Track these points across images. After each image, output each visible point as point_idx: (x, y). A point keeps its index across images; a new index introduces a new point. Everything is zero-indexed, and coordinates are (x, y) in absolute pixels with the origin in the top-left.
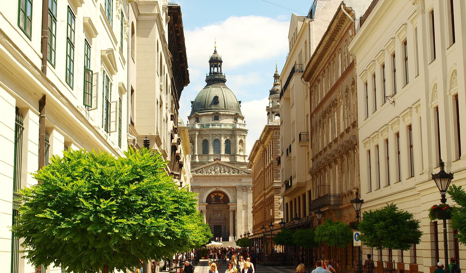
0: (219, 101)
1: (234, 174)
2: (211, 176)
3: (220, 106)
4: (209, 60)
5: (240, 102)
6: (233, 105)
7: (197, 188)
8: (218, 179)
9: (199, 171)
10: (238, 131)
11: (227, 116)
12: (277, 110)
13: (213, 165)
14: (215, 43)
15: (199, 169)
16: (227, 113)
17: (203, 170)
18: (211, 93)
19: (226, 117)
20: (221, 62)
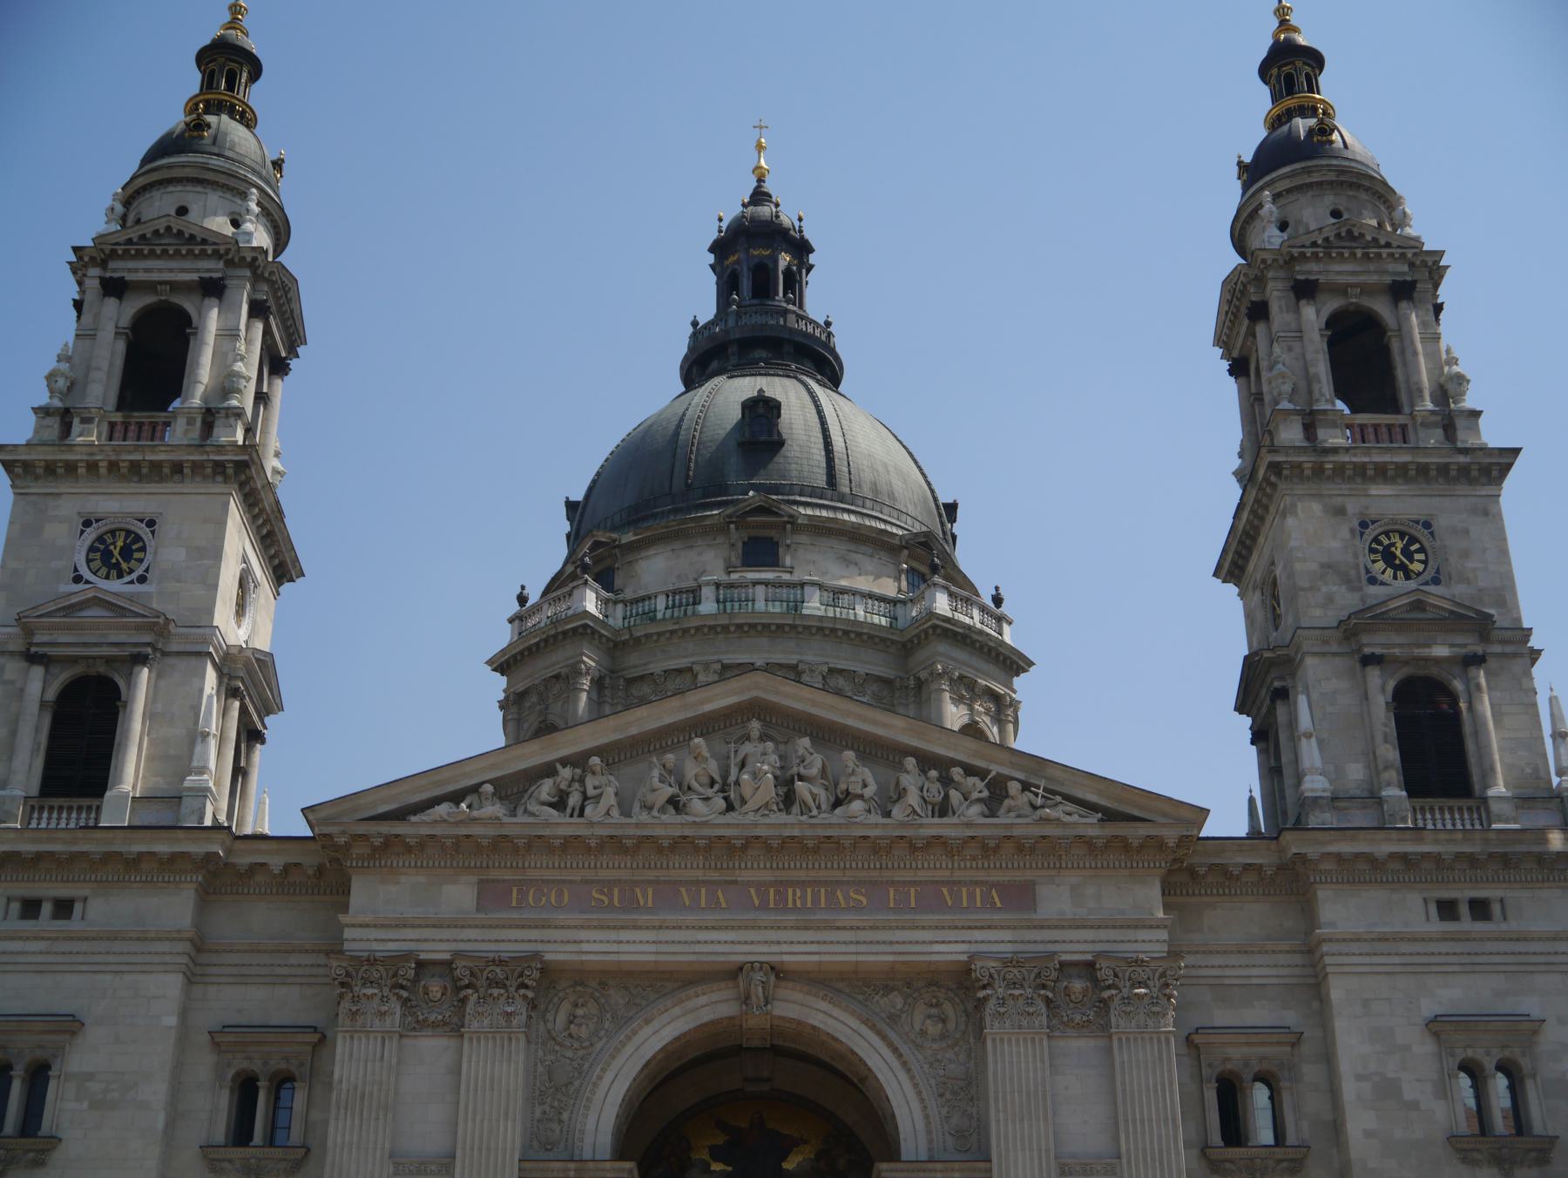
0: (785, 436)
1: (945, 820)
2: (681, 845)
3: (794, 473)
4: (713, 235)
5: (951, 509)
6: (898, 485)
7: (513, 984)
8: (761, 886)
9: (546, 789)
10: (942, 647)
11: (852, 547)
12: (1337, 267)
13: (705, 725)
14: (760, 147)
15: (549, 770)
16: (853, 518)
17: (590, 782)
18: (720, 399)
19: (842, 546)
20: (802, 248)
